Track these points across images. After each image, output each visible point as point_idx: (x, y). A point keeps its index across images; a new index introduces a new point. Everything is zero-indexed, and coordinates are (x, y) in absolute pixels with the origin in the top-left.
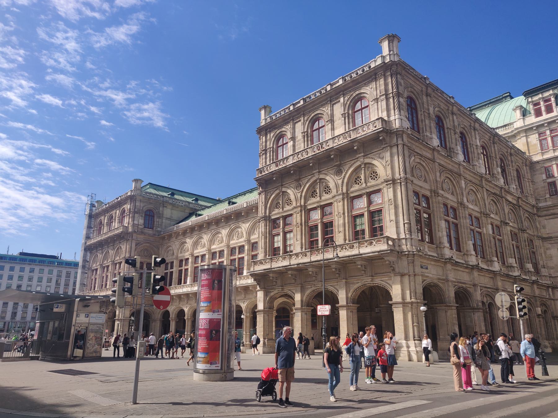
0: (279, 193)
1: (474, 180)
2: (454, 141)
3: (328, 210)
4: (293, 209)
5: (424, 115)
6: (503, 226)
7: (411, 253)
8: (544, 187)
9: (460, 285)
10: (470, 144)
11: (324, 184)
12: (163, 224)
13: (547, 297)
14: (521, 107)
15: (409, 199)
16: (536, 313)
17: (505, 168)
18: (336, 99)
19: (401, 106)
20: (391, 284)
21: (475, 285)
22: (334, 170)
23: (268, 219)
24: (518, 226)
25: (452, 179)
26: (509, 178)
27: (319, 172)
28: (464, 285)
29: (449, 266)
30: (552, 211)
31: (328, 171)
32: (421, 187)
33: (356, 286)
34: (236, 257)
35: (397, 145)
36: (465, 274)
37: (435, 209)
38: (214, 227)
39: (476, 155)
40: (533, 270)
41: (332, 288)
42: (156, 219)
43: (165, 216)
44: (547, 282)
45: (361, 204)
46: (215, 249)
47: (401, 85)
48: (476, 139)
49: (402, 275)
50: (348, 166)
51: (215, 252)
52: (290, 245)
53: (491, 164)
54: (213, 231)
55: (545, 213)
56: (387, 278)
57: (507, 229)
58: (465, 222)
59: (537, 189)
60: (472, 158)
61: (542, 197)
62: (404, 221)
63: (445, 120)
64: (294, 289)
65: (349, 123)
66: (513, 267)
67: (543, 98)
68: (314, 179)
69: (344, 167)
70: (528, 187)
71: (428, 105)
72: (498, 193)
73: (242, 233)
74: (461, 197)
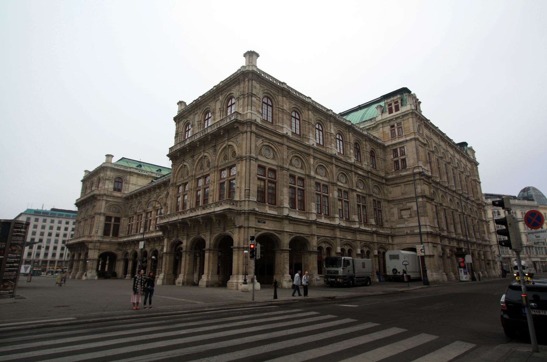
0: (182, 166)
1: (325, 159)
2: (307, 130)
5: (279, 110)
7: (246, 211)
8: (391, 164)
9: (298, 235)
12: (130, 188)
13: (387, 243)
14: (381, 106)
15: (251, 172)
16: (374, 254)
17: (359, 149)
19: (253, 103)
21: (312, 235)
24: (366, 192)
25: (302, 158)
26: (362, 157)
27: (204, 151)
28: (302, 235)
31: (209, 151)
32: (268, 163)
33: (216, 235)
35: (247, 132)
39: (329, 140)
42: (124, 185)
44: (387, 232)
45: (225, 174)
47: (255, 88)
48: (331, 128)
49: (240, 227)
50: (219, 147)
53: (346, 147)
55: (391, 183)
58: (311, 188)
59: (388, 165)
61: (390, 171)
62: (245, 187)
63: (301, 114)
67: (393, 100)
70: (380, 164)
71: (283, 103)
72: (349, 168)
74: (309, 171)
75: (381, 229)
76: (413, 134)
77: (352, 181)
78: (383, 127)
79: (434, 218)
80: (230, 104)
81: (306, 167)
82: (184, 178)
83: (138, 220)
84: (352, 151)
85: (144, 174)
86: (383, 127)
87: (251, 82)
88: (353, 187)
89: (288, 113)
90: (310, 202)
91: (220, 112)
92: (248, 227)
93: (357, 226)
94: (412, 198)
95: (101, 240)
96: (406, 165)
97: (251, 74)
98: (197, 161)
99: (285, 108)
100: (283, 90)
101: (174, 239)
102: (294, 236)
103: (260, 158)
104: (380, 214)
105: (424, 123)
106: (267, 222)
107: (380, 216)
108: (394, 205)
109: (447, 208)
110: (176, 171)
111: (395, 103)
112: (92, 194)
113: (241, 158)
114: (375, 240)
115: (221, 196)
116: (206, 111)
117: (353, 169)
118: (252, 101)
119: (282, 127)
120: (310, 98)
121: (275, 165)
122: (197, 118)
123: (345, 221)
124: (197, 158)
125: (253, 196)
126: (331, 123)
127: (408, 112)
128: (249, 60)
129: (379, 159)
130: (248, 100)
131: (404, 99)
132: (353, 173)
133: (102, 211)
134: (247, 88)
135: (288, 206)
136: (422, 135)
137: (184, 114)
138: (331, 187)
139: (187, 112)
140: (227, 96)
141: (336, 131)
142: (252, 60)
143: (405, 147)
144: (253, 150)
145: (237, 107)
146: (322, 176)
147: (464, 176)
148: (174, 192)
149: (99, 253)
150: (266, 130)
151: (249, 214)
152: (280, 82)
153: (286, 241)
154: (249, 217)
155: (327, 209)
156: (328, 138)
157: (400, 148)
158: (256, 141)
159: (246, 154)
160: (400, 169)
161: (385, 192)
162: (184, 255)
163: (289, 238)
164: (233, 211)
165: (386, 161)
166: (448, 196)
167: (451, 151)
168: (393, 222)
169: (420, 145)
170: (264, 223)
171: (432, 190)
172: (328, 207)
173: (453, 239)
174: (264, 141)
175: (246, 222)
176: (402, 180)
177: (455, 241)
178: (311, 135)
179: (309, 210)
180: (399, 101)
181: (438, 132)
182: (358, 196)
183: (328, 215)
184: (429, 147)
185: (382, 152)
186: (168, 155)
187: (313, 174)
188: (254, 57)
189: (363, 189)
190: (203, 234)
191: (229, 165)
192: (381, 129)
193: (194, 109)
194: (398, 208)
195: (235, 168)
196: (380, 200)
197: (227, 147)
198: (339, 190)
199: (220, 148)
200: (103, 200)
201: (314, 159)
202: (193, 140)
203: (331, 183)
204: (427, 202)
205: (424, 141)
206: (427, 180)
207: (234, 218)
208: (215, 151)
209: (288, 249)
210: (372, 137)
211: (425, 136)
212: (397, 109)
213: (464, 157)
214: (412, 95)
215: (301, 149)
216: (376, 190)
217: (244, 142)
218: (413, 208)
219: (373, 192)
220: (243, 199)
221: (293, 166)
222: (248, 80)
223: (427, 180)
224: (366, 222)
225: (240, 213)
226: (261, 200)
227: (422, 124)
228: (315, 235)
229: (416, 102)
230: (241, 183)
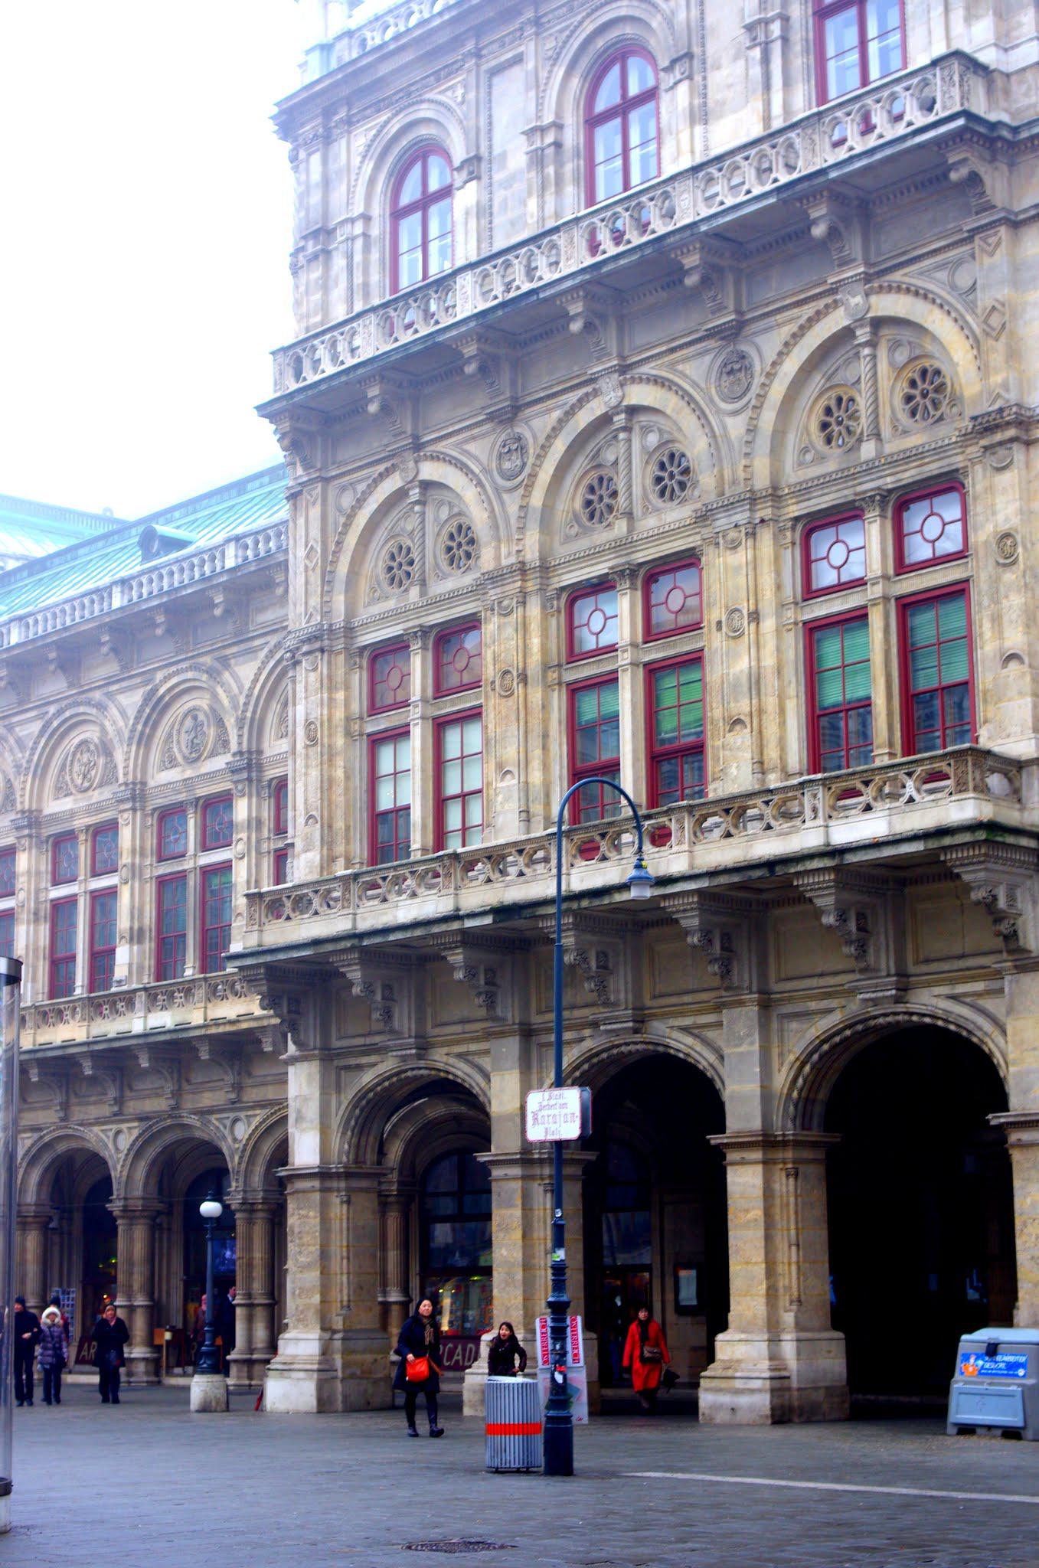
0: (400, 494)
3: (672, 596)
4: (478, 589)
11: (653, 439)
20: (721, 1043)
22: (708, 358)
23: (340, 645)
27: (623, 369)
31: (672, 366)
34: (188, 865)
41: (689, 1040)
46: (72, 814)
50: (786, 332)
51: (70, 836)
52: (464, 797)
54: (52, 709)
56: (979, 986)
64: (486, 1052)
65: (787, 83)
68: (595, 409)
69: (759, 340)
73: (220, 723)
82: (423, 583)
91: (757, 53)
98: (560, 447)
101: (387, 1065)
110: (344, 533)
116: (600, 43)
124: (556, 431)
137: (384, 69)
139: (408, 57)
148: (340, 696)
162: (517, 1185)
186: (267, 411)
190: (688, 1021)
191: (889, 482)
193: (478, 31)
207: (1011, 898)
208: (736, 368)
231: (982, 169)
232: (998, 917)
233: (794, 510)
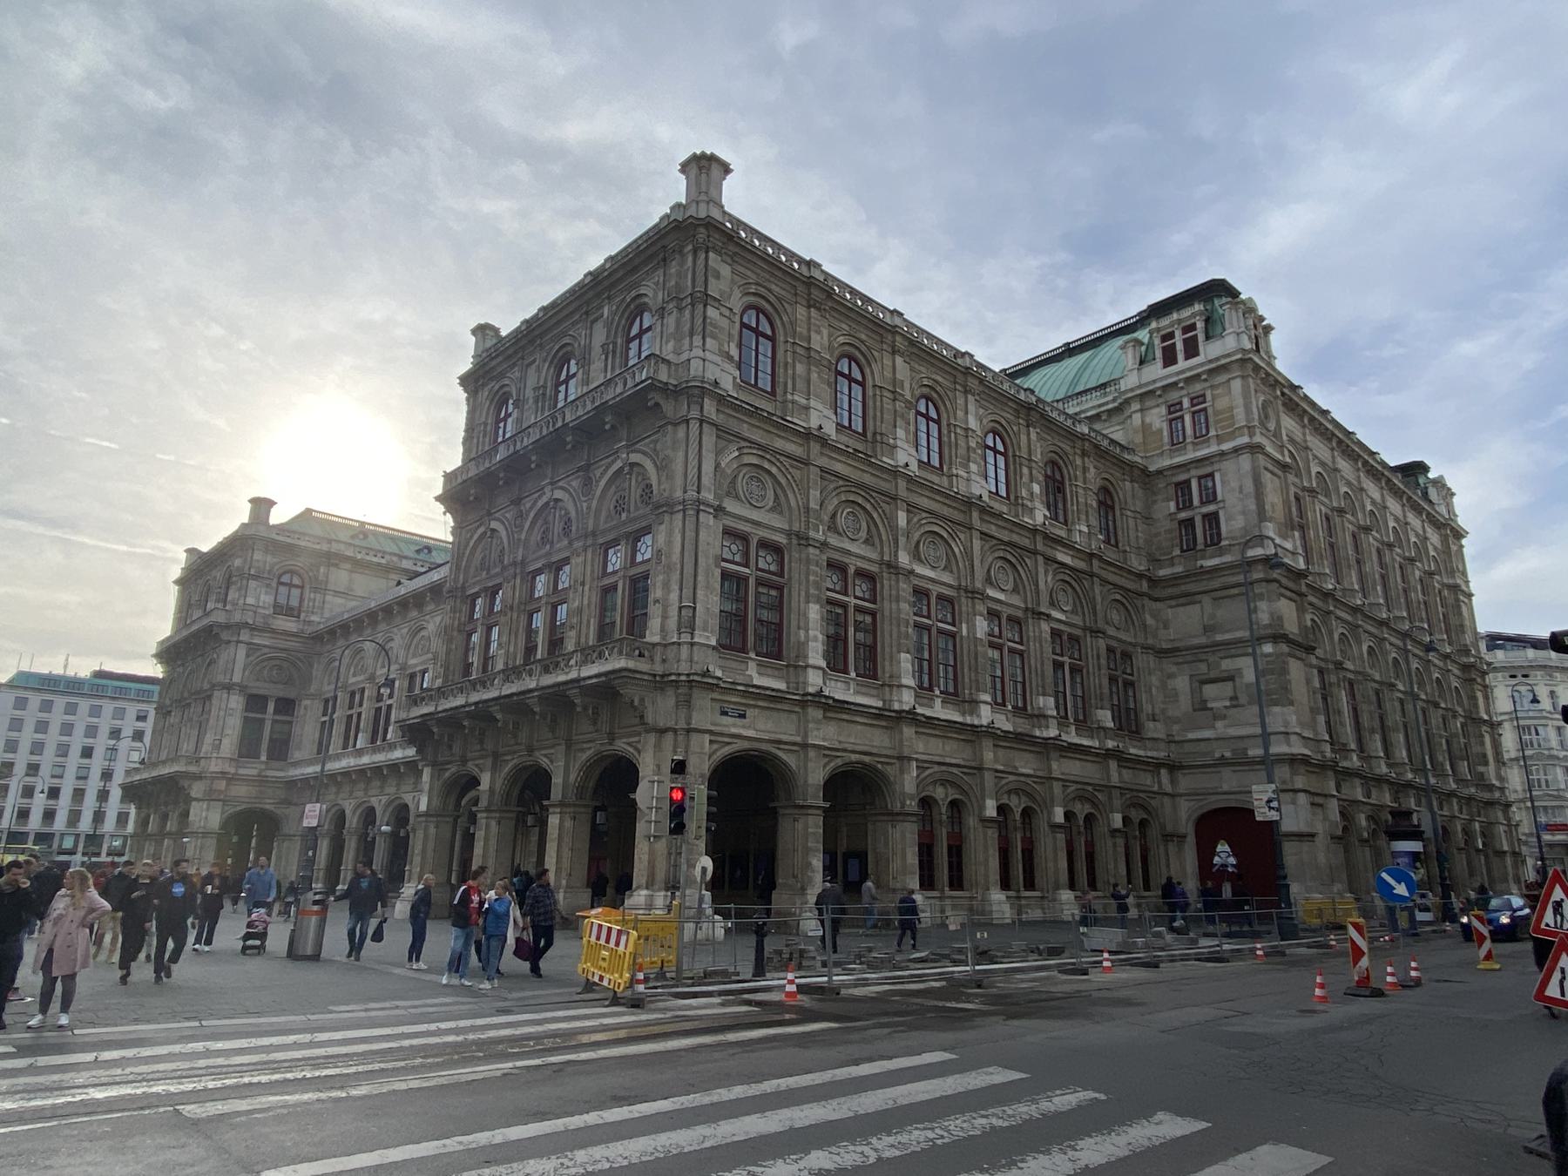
0: (485, 533)
1: (946, 511)
2: (888, 417)
5: (794, 352)
6: (1030, 621)
7: (683, 678)
8: (1169, 531)
9: (854, 757)
10: (949, 425)
14: (1139, 343)
16: (1109, 825)
17: (1062, 483)
18: (598, 309)
19: (709, 328)
24: (1084, 621)
25: (868, 507)
26: (1072, 508)
28: (867, 759)
29: (815, 713)
30: (1183, 588)
33: (584, 756)
35: (687, 421)
36: (877, 732)
37: (796, 576)
38: (414, 614)
39: (962, 451)
40: (1111, 724)
43: (331, 587)
44: (1154, 754)
45: (616, 560)
47: (718, 276)
48: (967, 413)
53: (1015, 474)
55: (1170, 591)
57: (1040, 628)
58: (900, 608)
59: (1159, 534)
60: (951, 457)
61: (1164, 554)
66: (1045, 717)
67: (1179, 321)
70: (1132, 530)
71: (809, 330)
72: (1026, 542)
75: (1135, 743)
76: (1246, 430)
77: (1037, 585)
78: (1141, 410)
79: (1314, 711)
80: (635, 331)
81: (884, 538)
83: (351, 707)
84: (1036, 488)
85: (375, 560)
86: (1141, 410)
87: (703, 256)
88: (1038, 604)
89: (825, 363)
90: (894, 649)
92: (689, 731)
93: (1052, 732)
94: (1240, 641)
95: (233, 771)
96: (1219, 534)
97: (702, 230)
98: (532, 515)
99: (815, 345)
100: (810, 282)
101: (453, 769)
102: (839, 762)
103: (731, 506)
104: (1131, 693)
105: (1283, 394)
106: (749, 713)
107: (1131, 699)
108: (1177, 664)
109: (1360, 678)
111: (1186, 330)
112: (205, 622)
113: (666, 507)
114: (1115, 779)
115: (604, 631)
116: (560, 354)
117: (1040, 547)
118: (705, 318)
119: (807, 408)
120: (901, 315)
121: (781, 531)
122: (535, 377)
123: (1010, 716)
124: (531, 508)
125: (705, 629)
126: (970, 396)
127: (1228, 360)
128: (698, 184)
129: (1129, 513)
130: (693, 317)
131: (1215, 316)
132: (1040, 559)
133: (237, 678)
134: (690, 276)
135: (823, 664)
136: (1274, 436)
138: (964, 604)
139: (500, 358)
140: (628, 305)
141: (985, 421)
142: (708, 183)
143: (1217, 476)
144: (706, 480)
145: (658, 339)
146: (934, 568)
147: (1417, 573)
149: (223, 813)
150: (755, 412)
151: (691, 688)
152: (801, 261)
153: (815, 775)
154: (690, 695)
155: (951, 676)
156: (956, 444)
157: (1200, 478)
158: (719, 453)
159: (685, 492)
160: (1200, 546)
161: (1150, 621)
163: (824, 767)
164: (638, 676)
165: (1149, 521)
166: (1364, 636)
167: (1373, 490)
168: (1177, 721)
169: (1266, 469)
170: (743, 716)
171: (1308, 617)
172: (955, 667)
173: (1380, 780)
174: (745, 451)
175: (683, 714)
176: (1205, 583)
177: (1386, 787)
178: (900, 433)
179: (891, 677)
180: (1200, 325)
181: (1330, 427)
182: (1055, 633)
183: (956, 694)
184: (1298, 475)
185: (1140, 493)
186: (438, 499)
187: (904, 559)
188: (716, 171)
189: (1074, 612)
192: (1137, 418)
193: (523, 348)
194: (1191, 676)
195: (648, 539)
196: (1130, 649)
197: (626, 469)
198: (993, 615)
199: (602, 474)
200: (238, 642)
201: (908, 511)
202: (518, 447)
203: (966, 591)
204: (1290, 655)
205: (1283, 455)
206: (1291, 585)
208: (588, 483)
209: (821, 803)
210: (1105, 443)
211: (1285, 438)
212: (1192, 349)
213: (1418, 510)
214: (1243, 302)
215: (867, 479)
216: (1115, 617)
217: (681, 454)
218: (1242, 676)
219: (1107, 623)
220: (675, 640)
221: (840, 534)
222: (695, 251)
223: (1291, 585)
224: (1081, 717)
225: (661, 683)
226: (733, 640)
227: (1276, 397)
228: (910, 759)
229: (1255, 326)
230: (666, 586)
231: (661, 403)
232: (635, 709)
233: (601, 541)
